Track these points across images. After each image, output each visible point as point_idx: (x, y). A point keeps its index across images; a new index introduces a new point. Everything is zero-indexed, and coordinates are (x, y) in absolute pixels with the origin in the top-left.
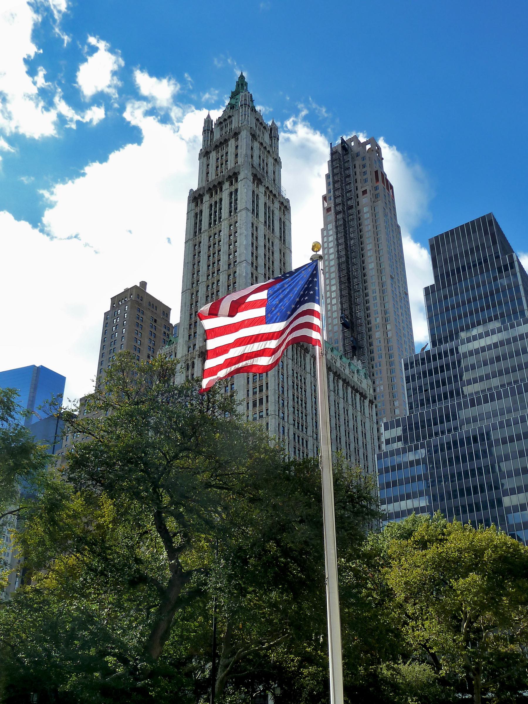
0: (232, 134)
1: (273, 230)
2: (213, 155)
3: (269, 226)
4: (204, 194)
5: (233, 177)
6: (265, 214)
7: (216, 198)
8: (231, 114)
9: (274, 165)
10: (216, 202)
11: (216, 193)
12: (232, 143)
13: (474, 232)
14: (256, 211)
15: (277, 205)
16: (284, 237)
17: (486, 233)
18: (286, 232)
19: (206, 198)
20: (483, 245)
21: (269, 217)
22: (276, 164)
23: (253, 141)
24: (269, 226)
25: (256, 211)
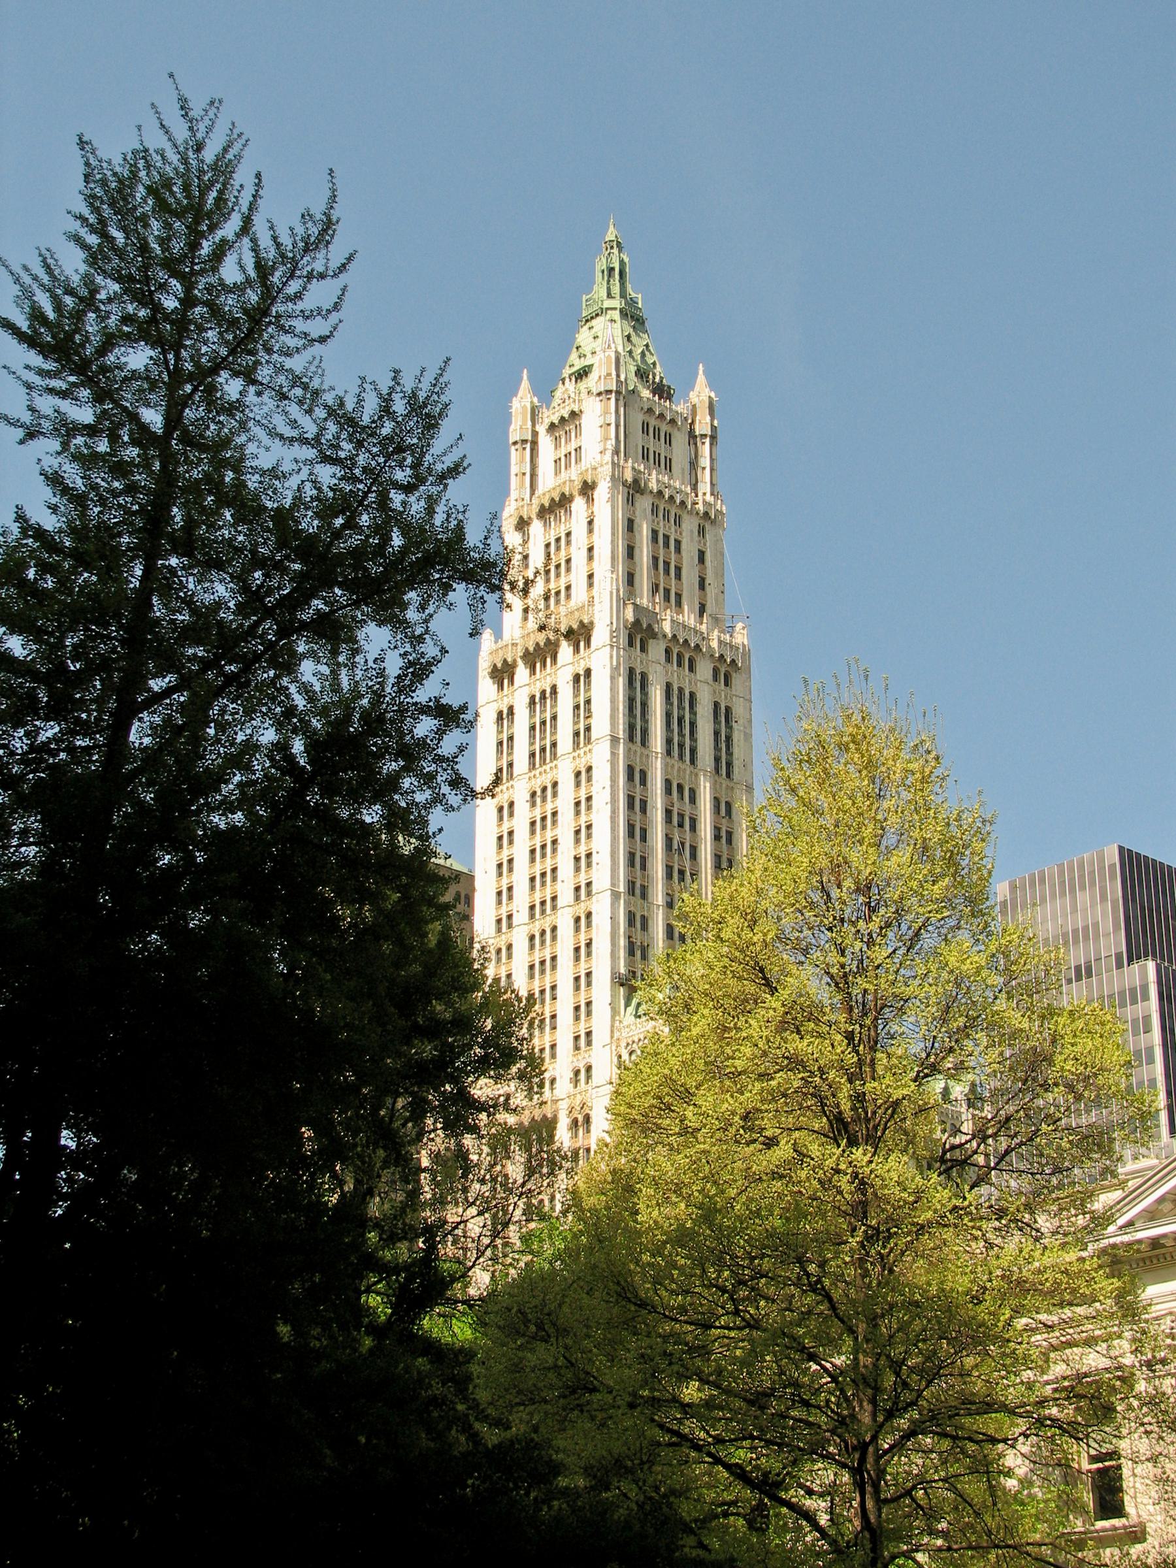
0: (578, 485)
1: (693, 751)
2: (536, 527)
3: (681, 746)
4: (515, 661)
5: (580, 635)
6: (668, 715)
7: (543, 681)
8: (576, 409)
9: (702, 531)
10: (543, 692)
11: (544, 665)
12: (579, 504)
13: (1082, 888)
14: (638, 728)
15: (704, 669)
16: (729, 753)
17: (1103, 898)
18: (736, 736)
19: (522, 672)
20: (1095, 925)
21: (681, 720)
22: (708, 527)
23: (630, 500)
24: (681, 746)
25: (638, 728)
